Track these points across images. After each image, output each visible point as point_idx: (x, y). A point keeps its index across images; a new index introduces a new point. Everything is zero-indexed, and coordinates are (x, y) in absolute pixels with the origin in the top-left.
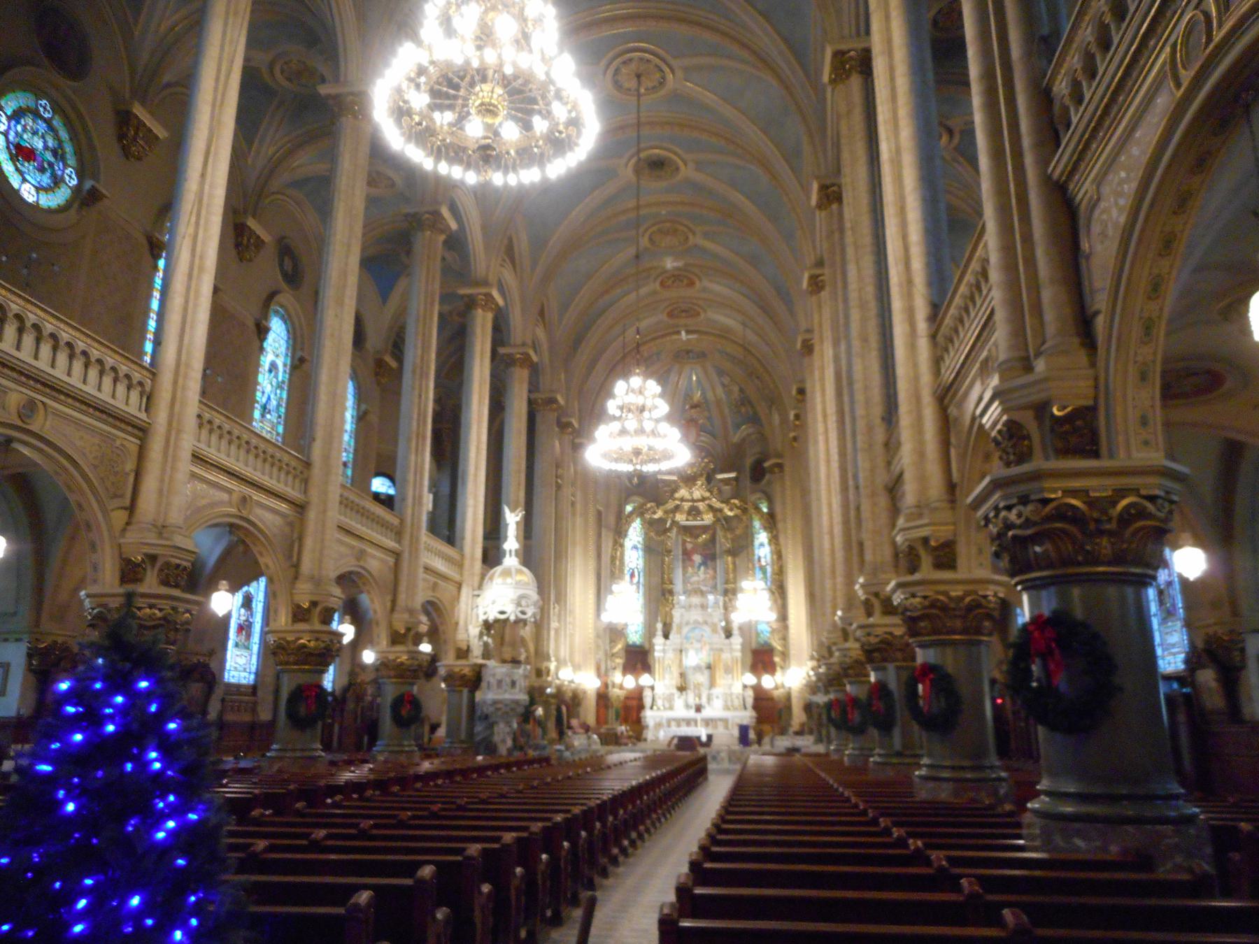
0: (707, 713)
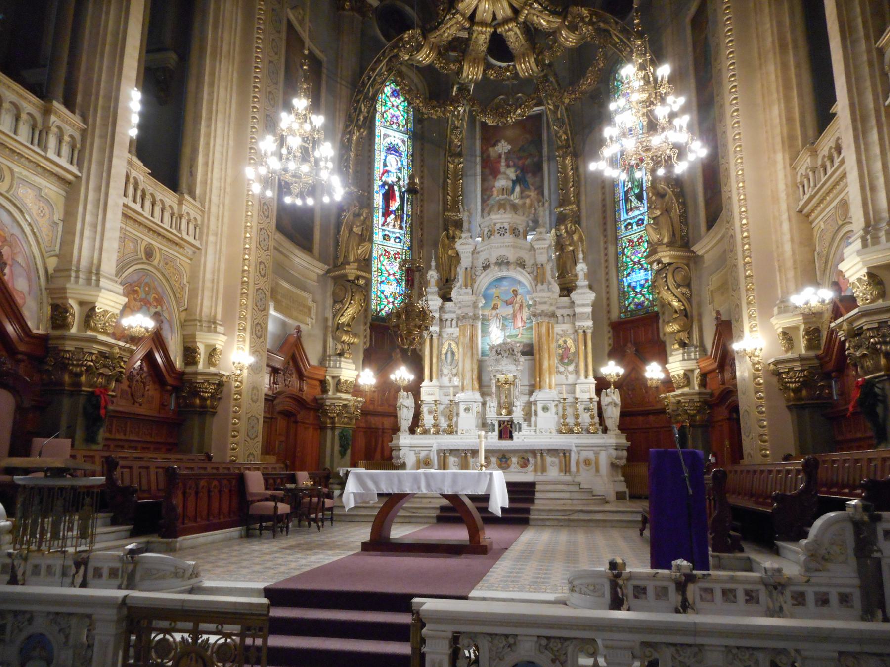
0: (523, 439)
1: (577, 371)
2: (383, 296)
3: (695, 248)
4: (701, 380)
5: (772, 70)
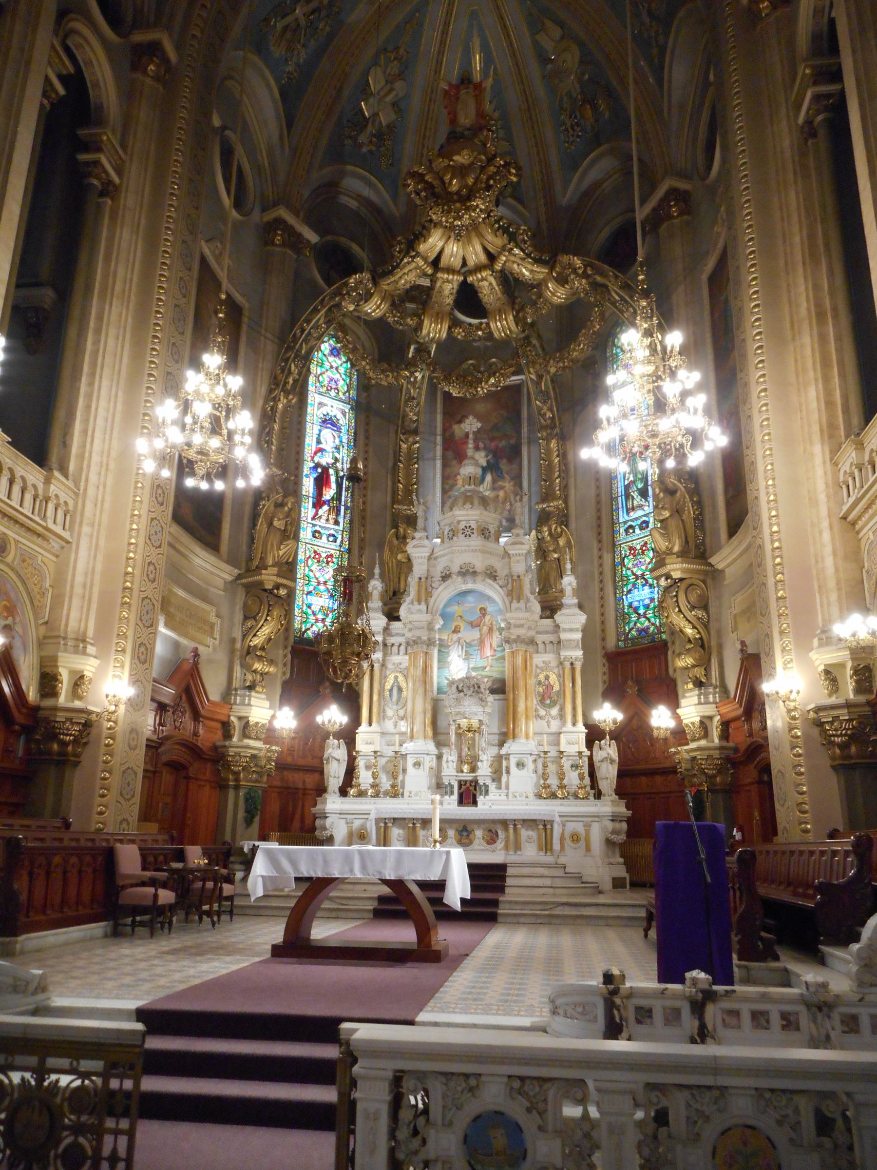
0: (490, 805)
1: (562, 716)
2: (309, 611)
3: (712, 561)
4: (722, 730)
5: (807, 342)
